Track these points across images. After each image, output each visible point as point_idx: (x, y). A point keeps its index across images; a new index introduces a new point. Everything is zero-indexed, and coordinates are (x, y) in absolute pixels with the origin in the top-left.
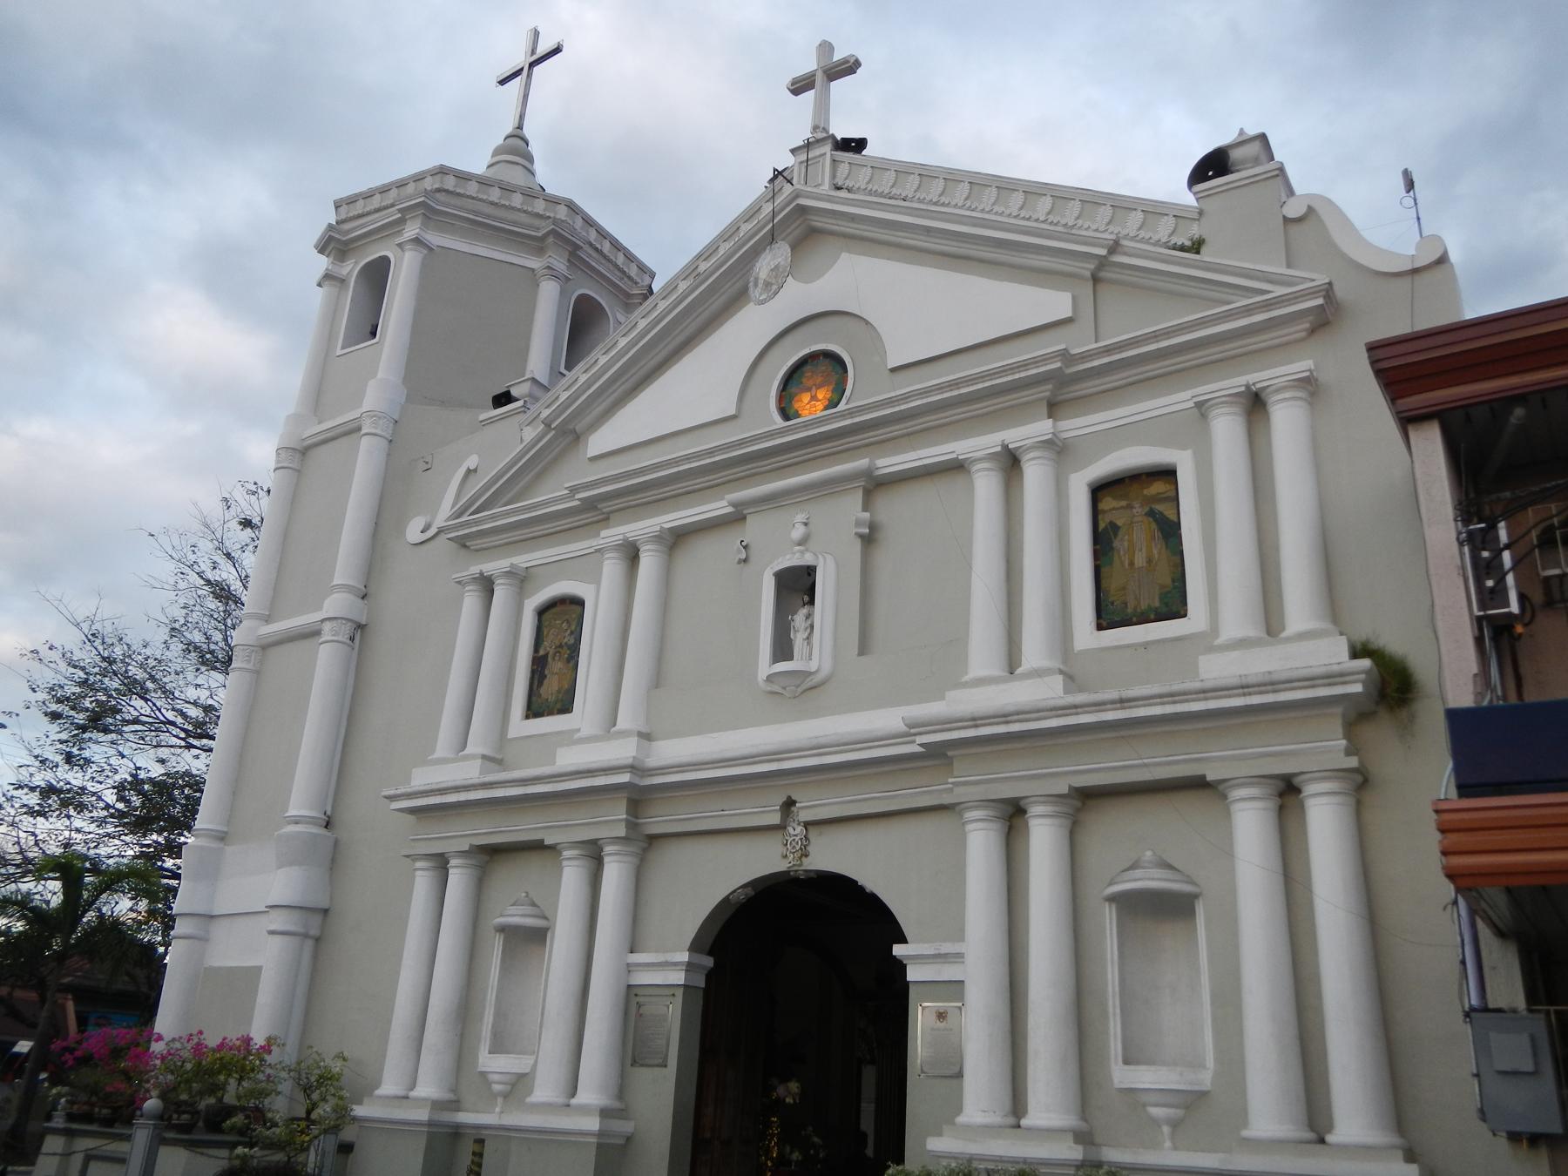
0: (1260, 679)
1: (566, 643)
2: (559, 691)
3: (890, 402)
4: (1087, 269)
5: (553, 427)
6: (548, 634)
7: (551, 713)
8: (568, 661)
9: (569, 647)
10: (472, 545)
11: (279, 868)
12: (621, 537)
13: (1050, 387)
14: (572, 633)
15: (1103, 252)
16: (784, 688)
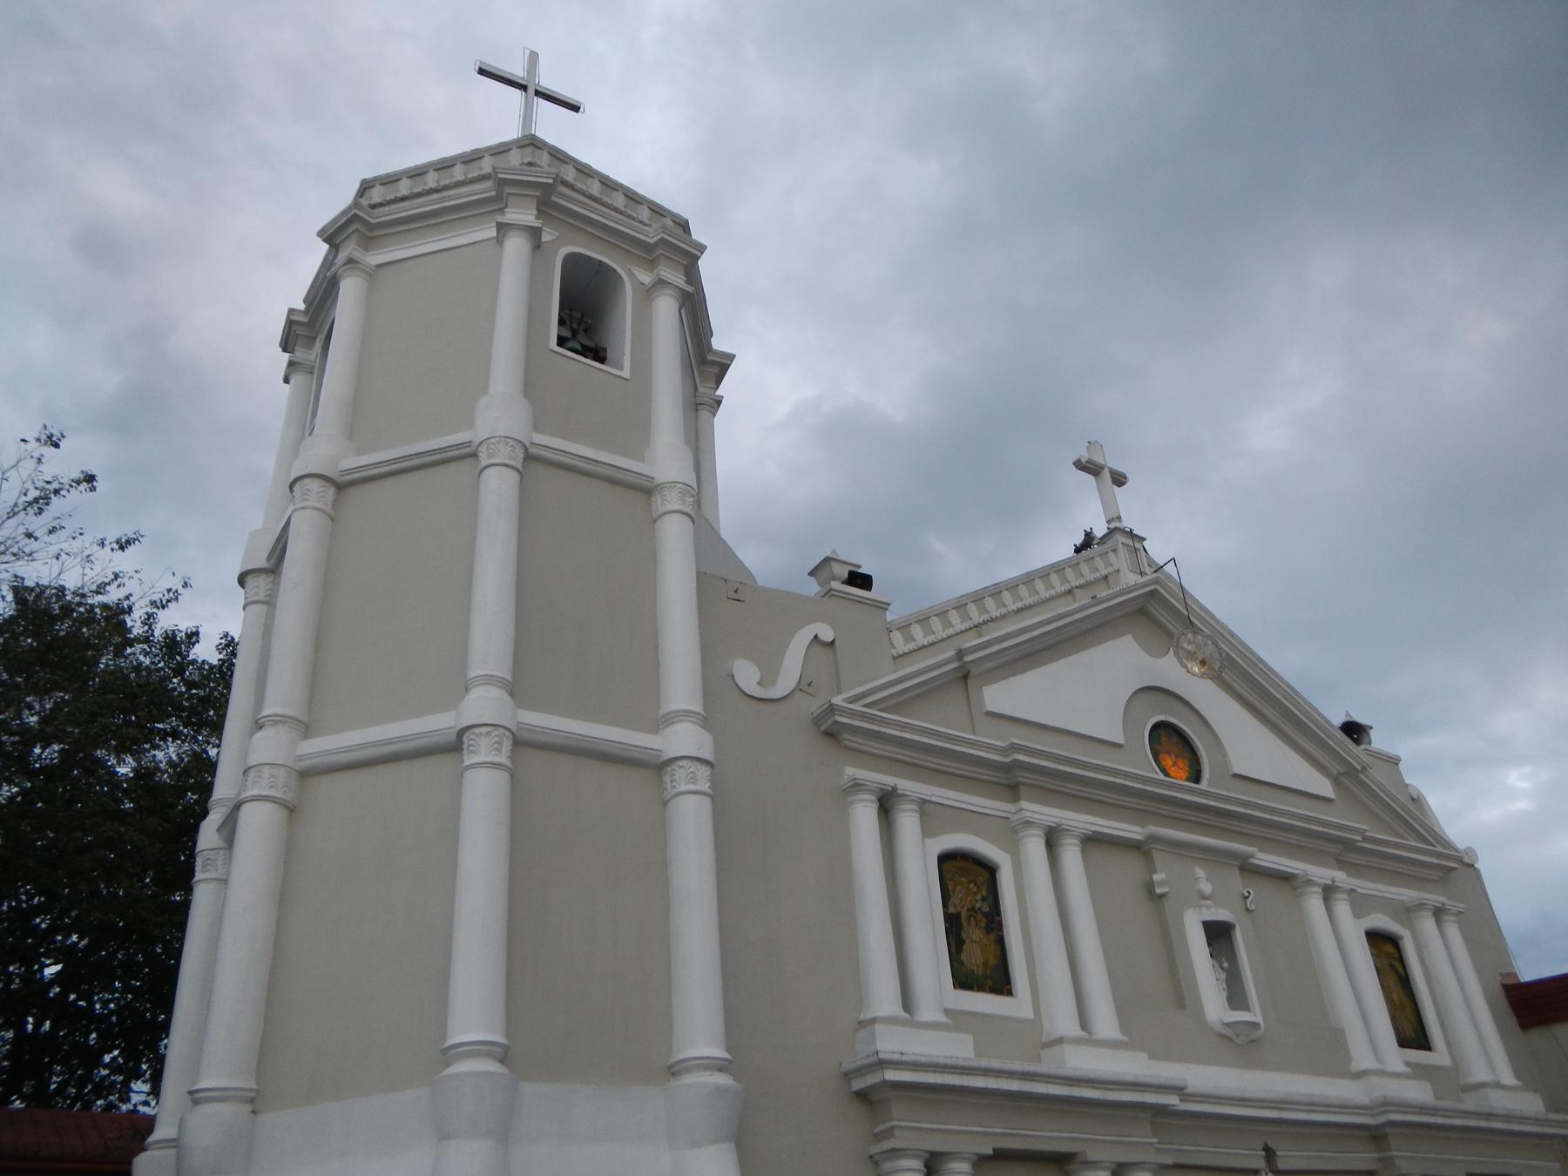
0: (1505, 1112)
1: (979, 909)
2: (985, 964)
3: (1273, 811)
4: (1336, 769)
5: (967, 659)
6: (954, 889)
7: (981, 988)
8: (988, 930)
9: (986, 915)
10: (848, 740)
11: (716, 1141)
12: (1056, 820)
13: (1341, 848)
14: (983, 899)
15: (1359, 768)
16: (1238, 1035)
